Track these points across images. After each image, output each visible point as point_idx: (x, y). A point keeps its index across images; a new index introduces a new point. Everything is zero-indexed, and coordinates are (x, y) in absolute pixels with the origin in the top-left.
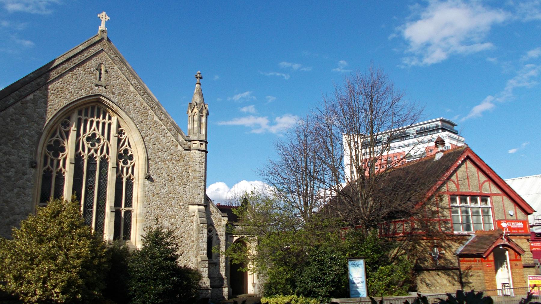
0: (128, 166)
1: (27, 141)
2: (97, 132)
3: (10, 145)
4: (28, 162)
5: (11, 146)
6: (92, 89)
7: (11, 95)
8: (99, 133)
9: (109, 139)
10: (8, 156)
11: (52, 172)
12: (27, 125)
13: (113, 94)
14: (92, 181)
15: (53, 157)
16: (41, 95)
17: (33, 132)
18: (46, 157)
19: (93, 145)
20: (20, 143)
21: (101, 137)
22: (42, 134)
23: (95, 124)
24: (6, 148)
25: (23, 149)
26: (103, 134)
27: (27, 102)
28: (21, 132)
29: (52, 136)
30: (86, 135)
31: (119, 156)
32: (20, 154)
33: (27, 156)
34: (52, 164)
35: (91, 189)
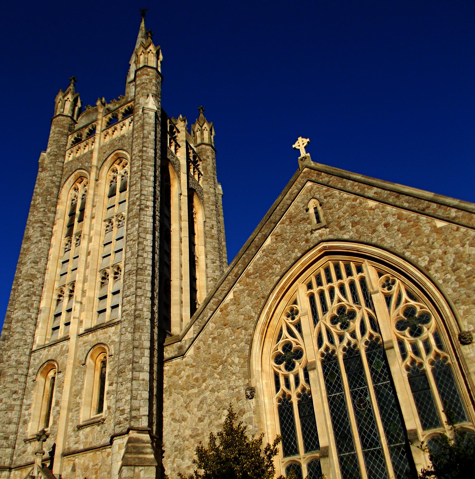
0: (424, 336)
1: (237, 360)
2: (345, 302)
3: (216, 375)
4: (243, 392)
5: (218, 377)
6: (307, 241)
7: (208, 307)
8: (348, 302)
9: (369, 303)
10: (216, 393)
11: (290, 397)
12: (233, 338)
13: (342, 228)
14: (362, 391)
15: (286, 372)
16: (242, 287)
17: (243, 344)
18: (277, 377)
19: (345, 326)
20: (229, 367)
21: (355, 307)
22: (252, 340)
23: (337, 291)
24: (212, 382)
25: (234, 374)
26: (356, 300)
27: (226, 306)
28: (228, 351)
29: (278, 340)
30: (328, 315)
31: (400, 326)
32: (232, 384)
33: (240, 383)
34: (288, 385)
35: (365, 406)
